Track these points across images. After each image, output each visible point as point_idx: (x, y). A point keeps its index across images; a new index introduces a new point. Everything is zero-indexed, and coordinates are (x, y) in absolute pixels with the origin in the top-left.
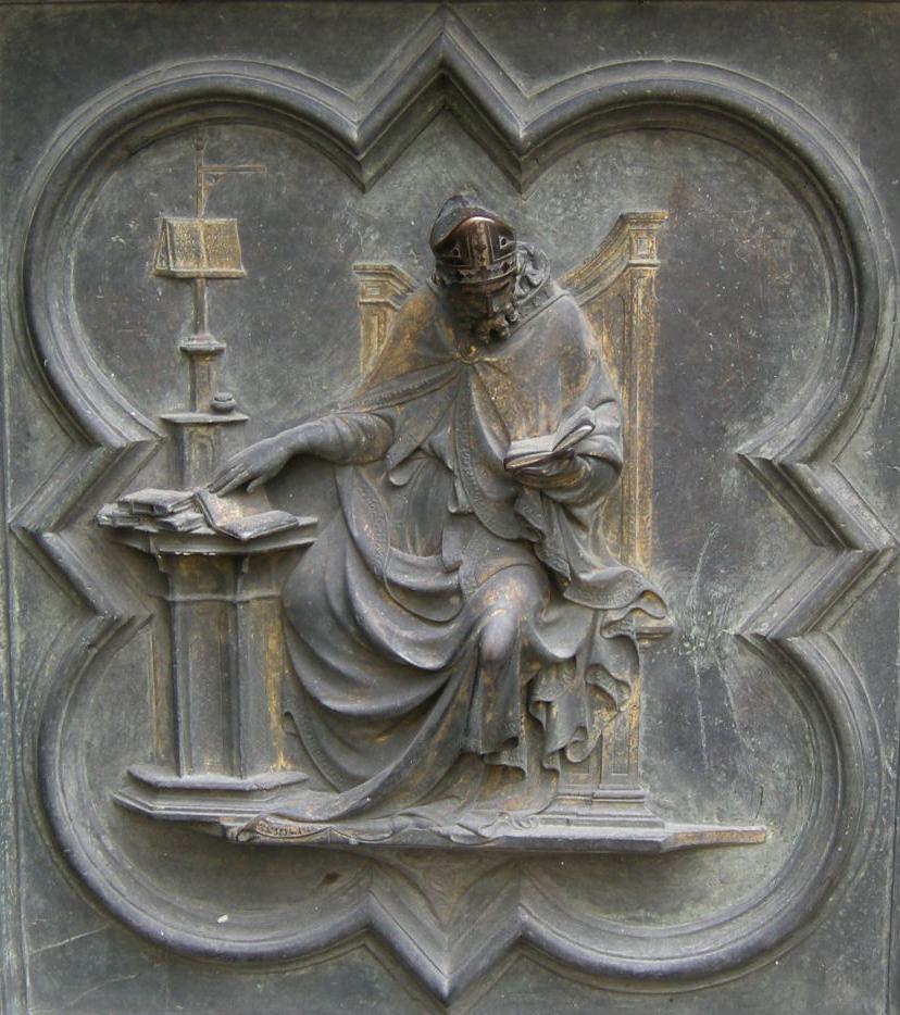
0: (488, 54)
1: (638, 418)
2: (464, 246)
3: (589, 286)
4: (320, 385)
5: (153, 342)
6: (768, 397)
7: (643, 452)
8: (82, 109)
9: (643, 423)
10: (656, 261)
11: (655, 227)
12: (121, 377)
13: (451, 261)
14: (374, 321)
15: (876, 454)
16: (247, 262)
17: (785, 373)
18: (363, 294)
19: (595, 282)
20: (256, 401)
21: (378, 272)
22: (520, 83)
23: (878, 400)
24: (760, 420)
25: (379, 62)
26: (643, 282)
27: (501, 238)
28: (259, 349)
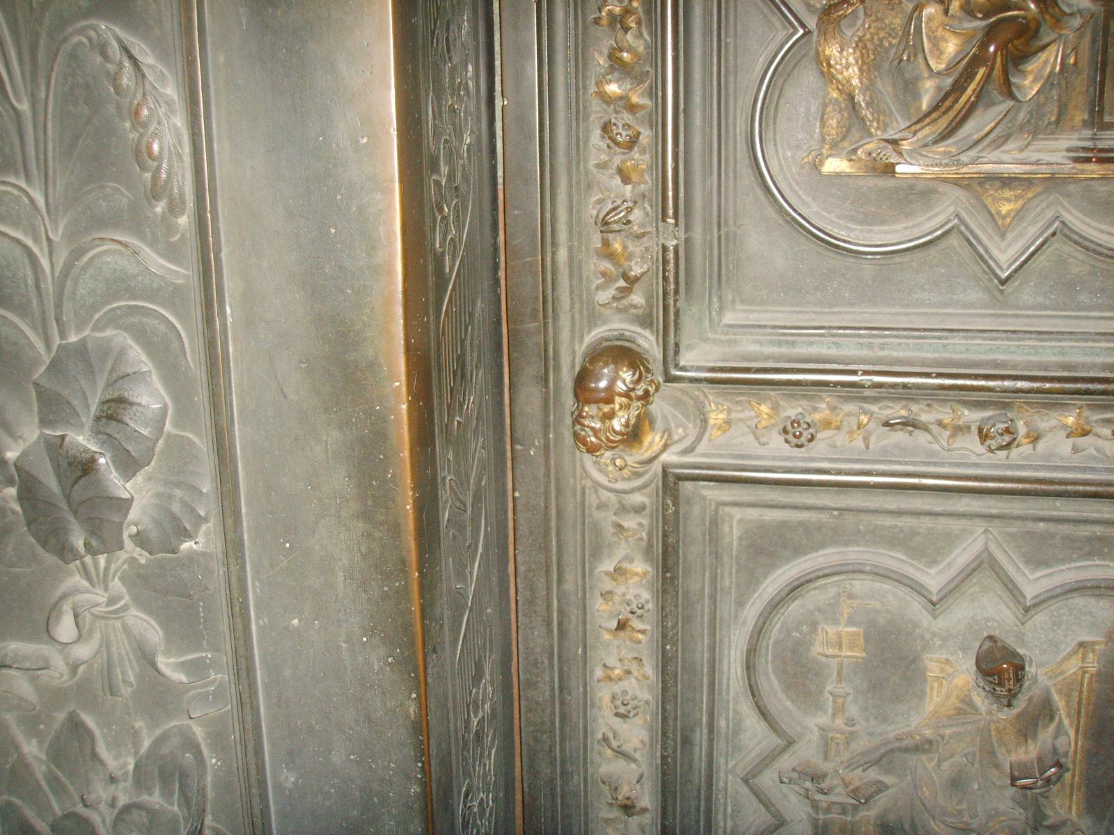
0: (1009, 556)
1: (1079, 744)
3: (1056, 676)
4: (903, 714)
5: (813, 688)
8: (778, 572)
9: (1082, 747)
10: (1096, 665)
11: (1097, 647)
12: (793, 702)
13: (991, 682)
14: (936, 685)
18: (931, 671)
19: (1060, 674)
20: (867, 720)
21: (939, 661)
22: (1026, 571)
28: (870, 695)
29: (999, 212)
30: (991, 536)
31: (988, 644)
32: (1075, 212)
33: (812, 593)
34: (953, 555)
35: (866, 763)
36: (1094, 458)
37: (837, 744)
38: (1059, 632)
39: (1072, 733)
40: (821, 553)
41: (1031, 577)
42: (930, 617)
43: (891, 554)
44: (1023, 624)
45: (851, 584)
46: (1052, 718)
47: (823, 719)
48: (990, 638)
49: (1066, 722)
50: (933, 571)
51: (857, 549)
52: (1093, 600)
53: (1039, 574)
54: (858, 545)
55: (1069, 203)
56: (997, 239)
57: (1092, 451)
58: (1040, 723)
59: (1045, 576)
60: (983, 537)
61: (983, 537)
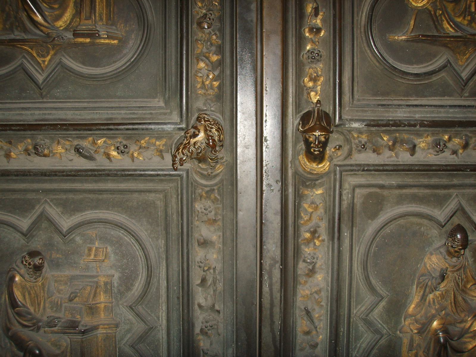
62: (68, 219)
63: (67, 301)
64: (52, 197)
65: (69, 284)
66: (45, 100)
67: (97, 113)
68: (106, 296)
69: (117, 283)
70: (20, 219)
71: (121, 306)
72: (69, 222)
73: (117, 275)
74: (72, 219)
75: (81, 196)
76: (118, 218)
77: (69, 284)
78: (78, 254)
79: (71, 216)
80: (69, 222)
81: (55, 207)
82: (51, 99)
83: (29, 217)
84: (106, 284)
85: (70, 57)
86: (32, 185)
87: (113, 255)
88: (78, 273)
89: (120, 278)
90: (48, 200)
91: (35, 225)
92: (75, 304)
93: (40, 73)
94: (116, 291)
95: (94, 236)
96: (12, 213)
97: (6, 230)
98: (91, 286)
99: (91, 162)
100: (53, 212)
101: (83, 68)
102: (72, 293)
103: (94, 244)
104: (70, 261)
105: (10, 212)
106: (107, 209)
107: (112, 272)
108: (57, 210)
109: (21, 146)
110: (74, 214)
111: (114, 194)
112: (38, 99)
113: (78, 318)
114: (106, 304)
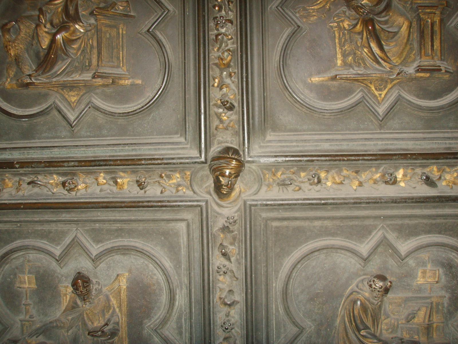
0: (87, 240)
1: (123, 319)
2: (76, 286)
3: (111, 290)
4: (53, 312)
6: (152, 314)
7: (125, 327)
12: (10, 310)
15: (177, 327)
16: (37, 285)
17: (156, 309)
19: (113, 289)
20: (39, 316)
22: (94, 246)
23: (176, 315)
24: (150, 319)
25: (64, 240)
26: (123, 289)
27: (85, 284)
28: (40, 304)
29: (71, 101)
30: (79, 231)
31: (77, 275)
32: (99, 100)
33: (14, 260)
34: (66, 240)
35: (37, 334)
36: (109, 194)
37: (27, 327)
38: (111, 271)
39: (120, 315)
40: (15, 243)
41: (96, 248)
42: (60, 268)
43: (42, 241)
44: (95, 268)
45: (28, 256)
46: (110, 309)
47: (22, 317)
48: (79, 273)
49: (117, 310)
50: (58, 248)
51: (29, 240)
52: (122, 257)
53: (99, 246)
54: (29, 239)
55: (97, 96)
56: (72, 111)
57: (109, 191)
58: (105, 311)
59: (101, 246)
60: (76, 232)
61: (76, 232)
62: (403, 243)
63: (404, 322)
64: (389, 222)
65: (403, 305)
66: (382, 131)
67: (436, 143)
68: (438, 317)
69: (447, 303)
70: (358, 244)
71: (450, 325)
72: (404, 246)
73: (448, 295)
74: (407, 243)
75: (416, 222)
76: (451, 241)
77: (403, 305)
78: (411, 276)
79: (406, 240)
80: (404, 246)
81: (391, 233)
82: (388, 130)
83: (366, 242)
84: (438, 304)
85: (405, 91)
86: (374, 211)
87: (444, 277)
88: (410, 295)
89: (450, 299)
90: (385, 226)
91: (374, 251)
92: (410, 324)
93: (377, 106)
94: (445, 310)
95: (427, 258)
96: (349, 239)
97: (342, 256)
98: (427, 307)
99: (433, 189)
100: (391, 237)
101: (418, 101)
102: (409, 315)
103: (426, 266)
104: (404, 283)
105: (347, 238)
106: (440, 233)
107: (443, 293)
108: (393, 235)
109: (364, 175)
110: (409, 239)
111: (447, 219)
112: (375, 130)
113: (416, 339)
114: (438, 324)
